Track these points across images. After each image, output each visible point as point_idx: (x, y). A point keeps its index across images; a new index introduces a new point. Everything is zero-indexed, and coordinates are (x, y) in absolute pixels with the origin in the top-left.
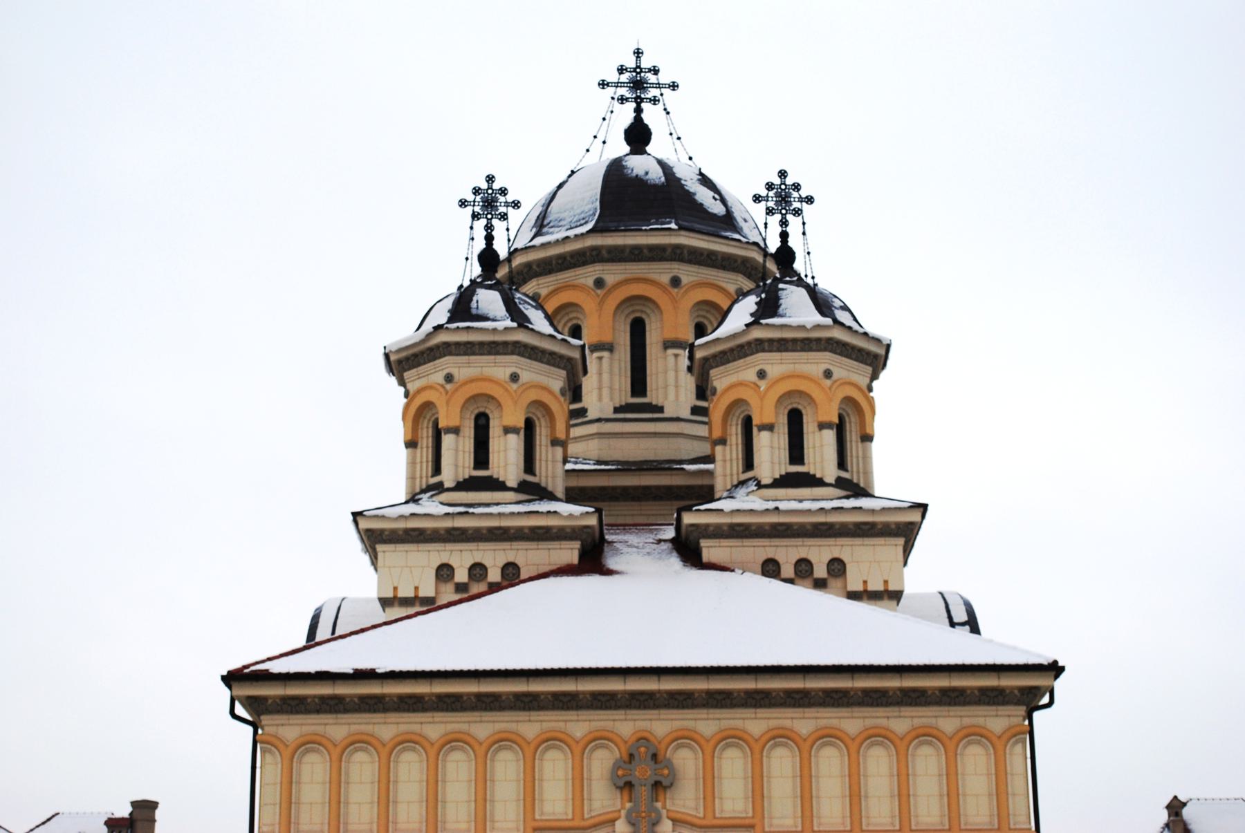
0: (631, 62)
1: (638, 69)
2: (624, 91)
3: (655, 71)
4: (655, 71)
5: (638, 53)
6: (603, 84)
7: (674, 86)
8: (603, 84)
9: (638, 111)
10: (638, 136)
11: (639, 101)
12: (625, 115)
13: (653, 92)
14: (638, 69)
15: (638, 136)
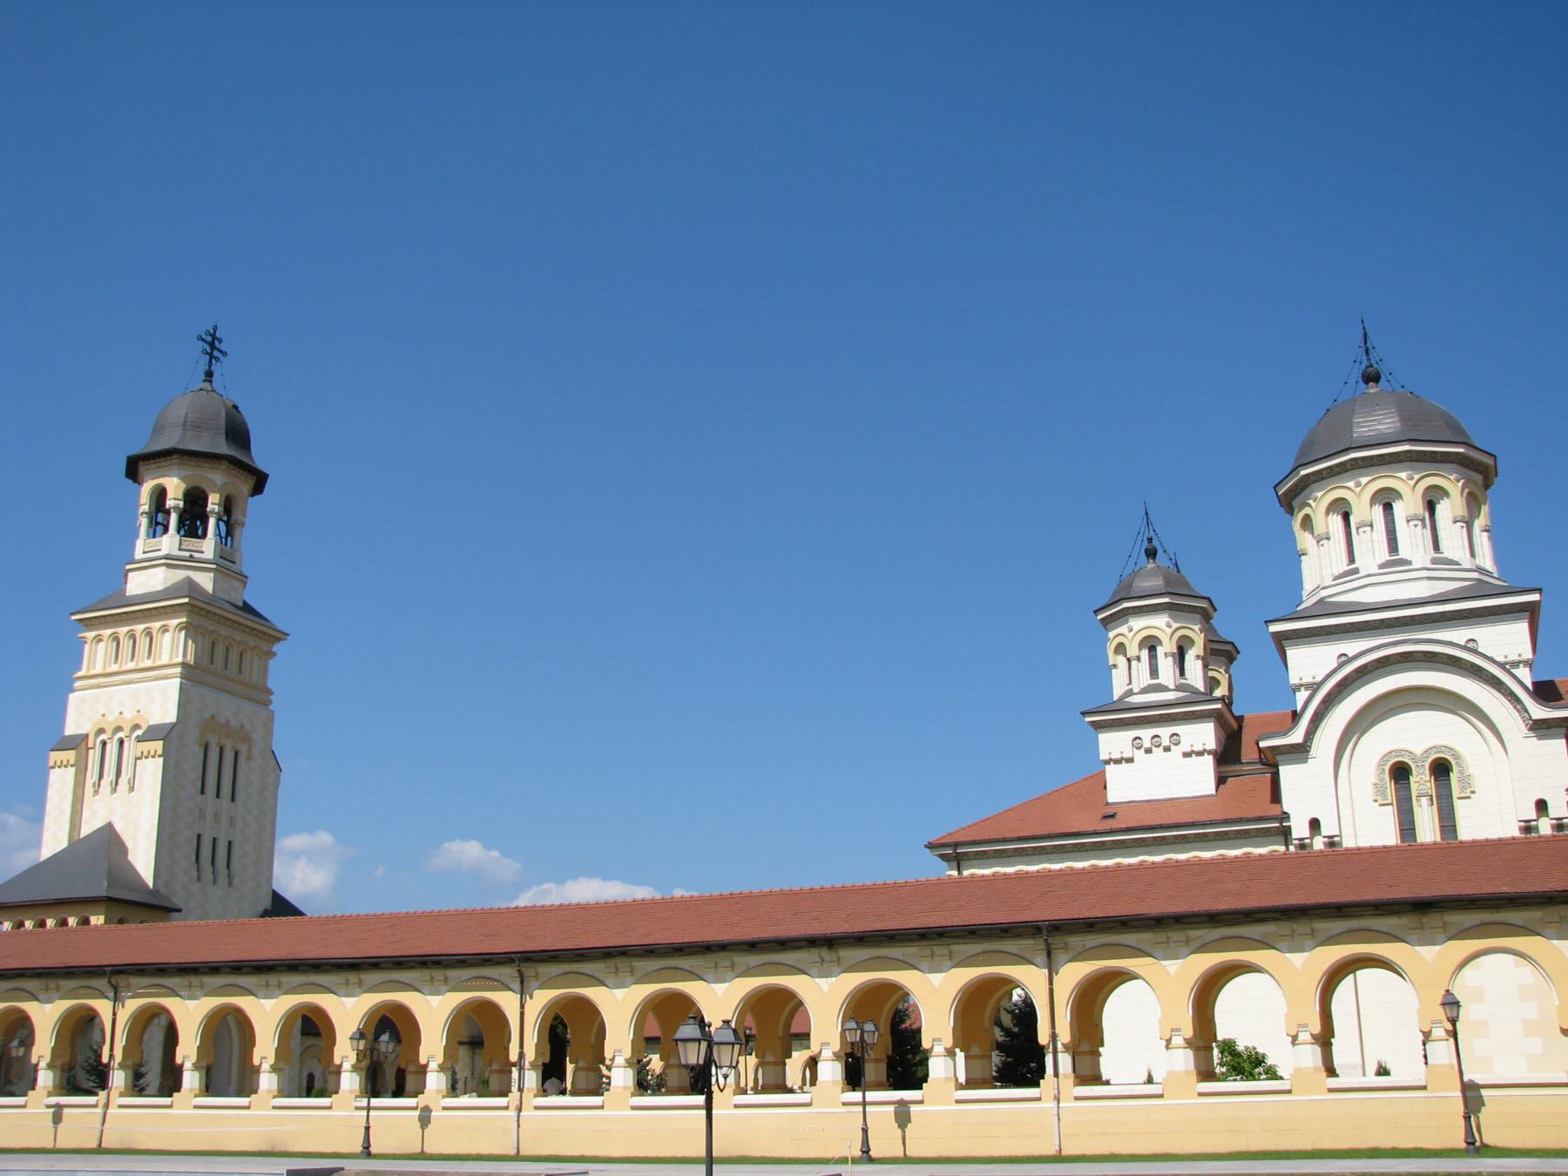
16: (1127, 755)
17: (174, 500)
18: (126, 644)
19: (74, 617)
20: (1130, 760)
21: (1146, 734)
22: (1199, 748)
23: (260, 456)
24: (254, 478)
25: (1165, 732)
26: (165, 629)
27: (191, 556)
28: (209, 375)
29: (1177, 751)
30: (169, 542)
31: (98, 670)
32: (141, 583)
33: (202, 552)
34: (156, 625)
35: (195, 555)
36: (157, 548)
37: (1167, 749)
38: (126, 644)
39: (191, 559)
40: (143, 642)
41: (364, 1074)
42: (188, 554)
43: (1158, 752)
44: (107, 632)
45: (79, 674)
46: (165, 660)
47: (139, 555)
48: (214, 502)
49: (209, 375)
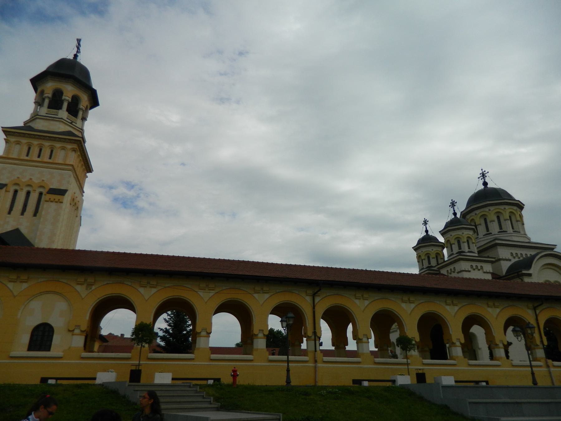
16: (469, 270)
18: (35, 151)
20: (470, 271)
21: (474, 264)
22: (488, 271)
25: (479, 264)
26: (63, 148)
29: (481, 271)
30: (63, 113)
31: (15, 156)
34: (58, 145)
36: (57, 114)
37: (479, 270)
38: (35, 151)
39: (71, 123)
40: (48, 152)
41: (197, 346)
43: (476, 270)
44: (24, 141)
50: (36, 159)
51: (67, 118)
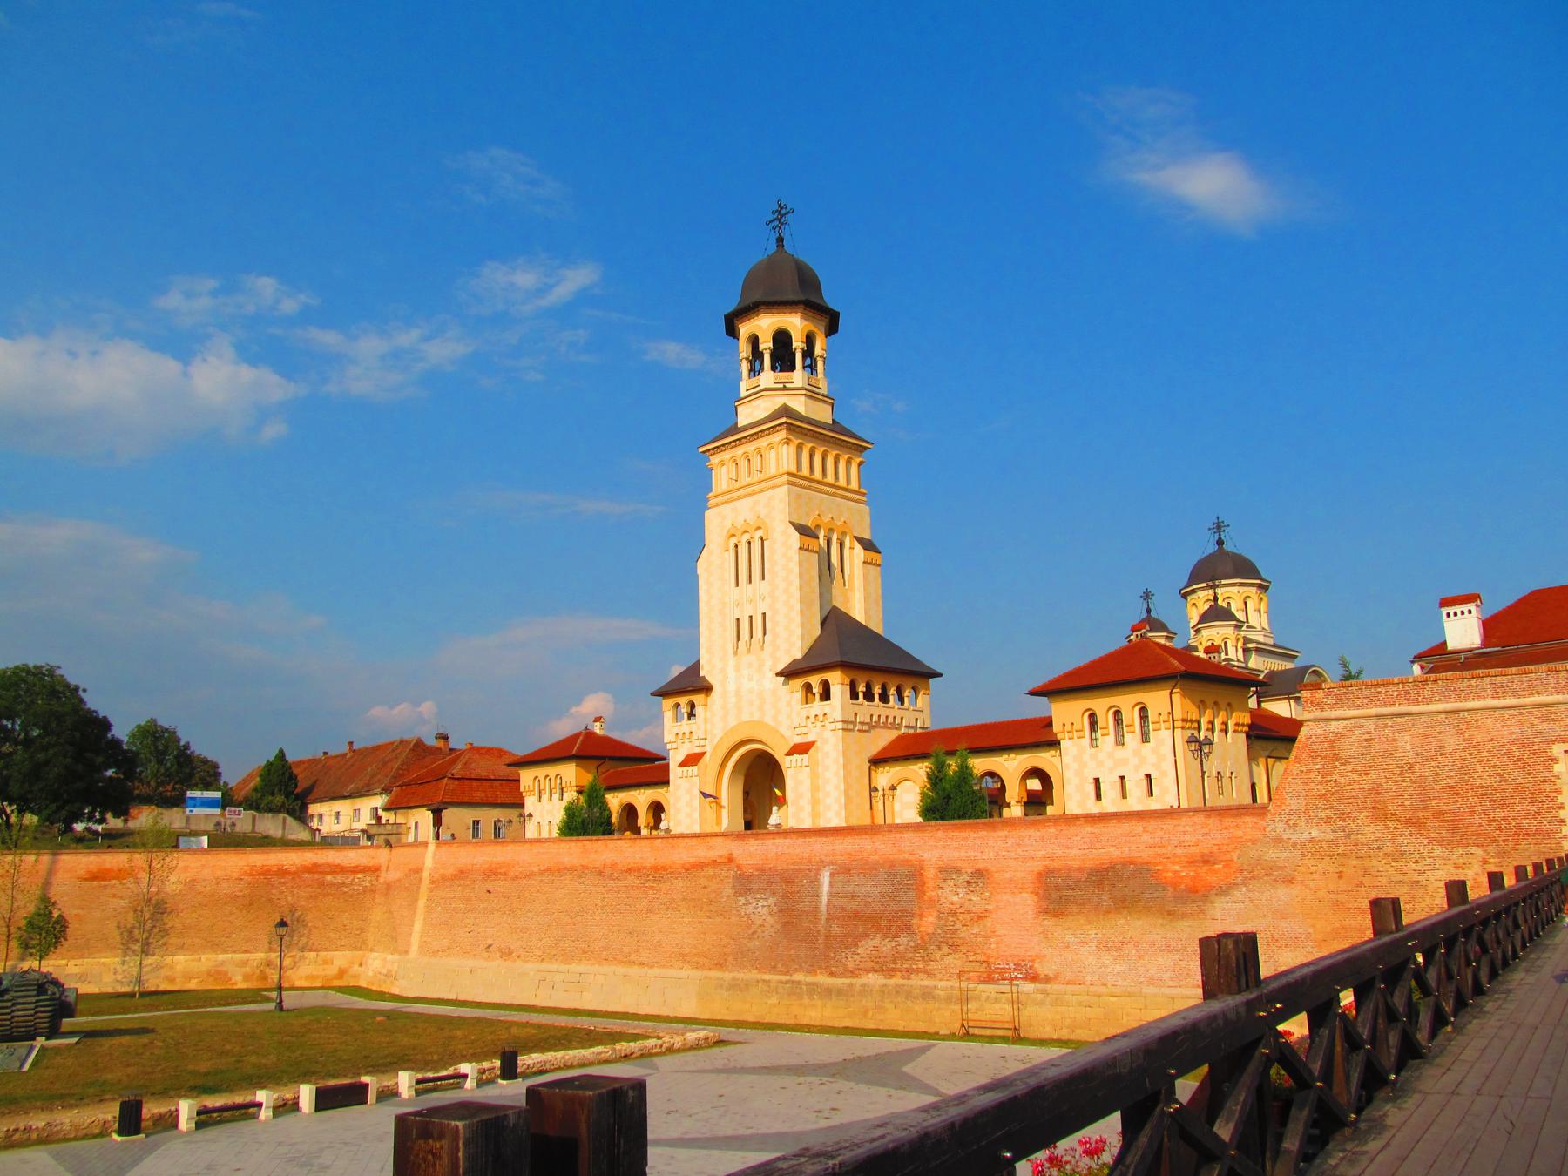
0: (1216, 521)
1: (1218, 523)
2: (1215, 530)
3: (1223, 522)
4: (1223, 522)
5: (1218, 518)
6: (1210, 529)
7: (1228, 526)
8: (1210, 529)
9: (1220, 535)
10: (1220, 543)
11: (1220, 532)
12: (1217, 536)
13: (1223, 529)
14: (1218, 523)
15: (1220, 543)
17: (766, 345)
19: (701, 450)
23: (831, 300)
24: (828, 317)
26: (770, 446)
27: (785, 386)
28: (780, 240)
30: (767, 378)
32: (747, 415)
33: (793, 382)
35: (787, 385)
39: (785, 388)
40: (756, 460)
42: (781, 386)
45: (711, 494)
46: (773, 471)
47: (743, 394)
48: (798, 344)
49: (780, 240)
50: (749, 480)
51: (775, 383)
